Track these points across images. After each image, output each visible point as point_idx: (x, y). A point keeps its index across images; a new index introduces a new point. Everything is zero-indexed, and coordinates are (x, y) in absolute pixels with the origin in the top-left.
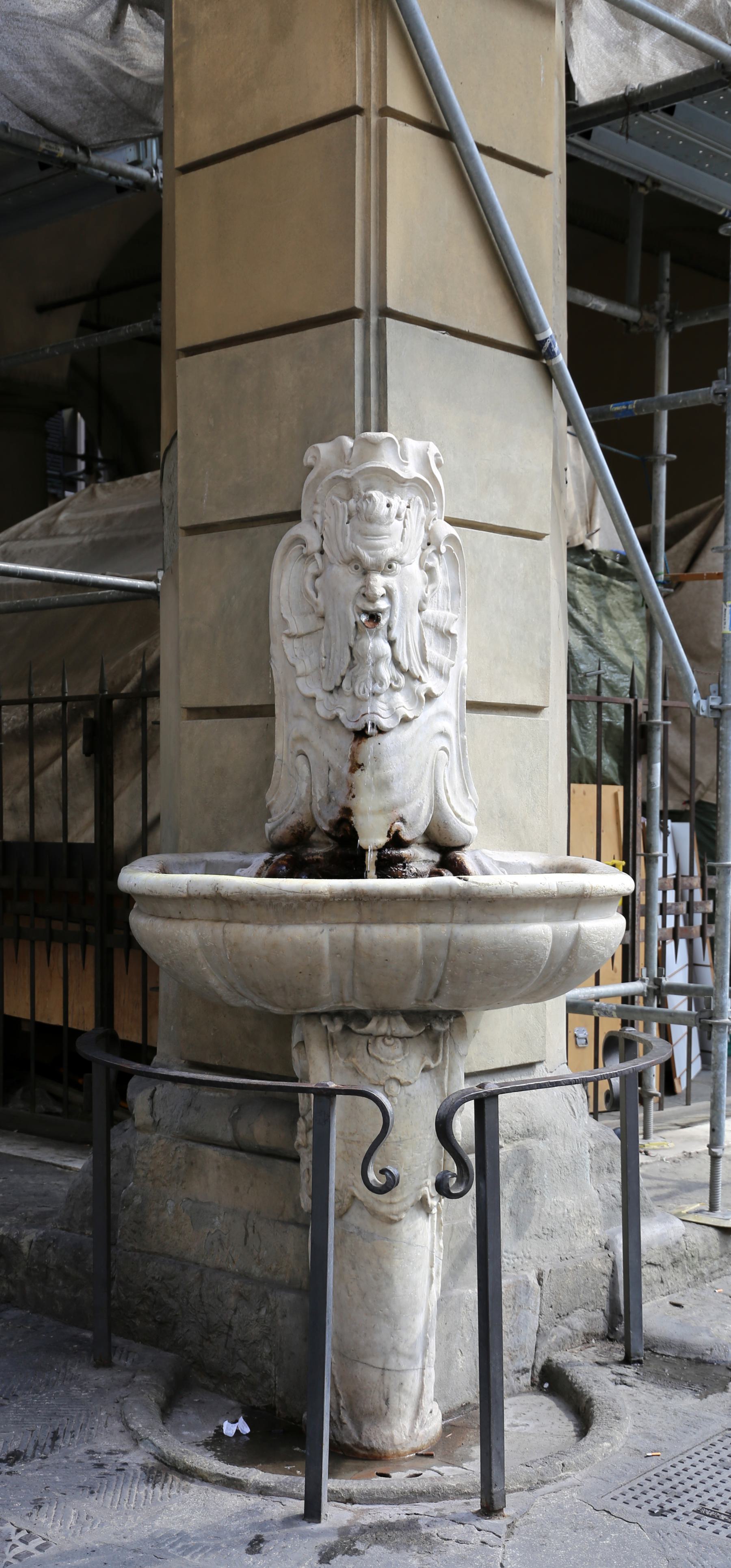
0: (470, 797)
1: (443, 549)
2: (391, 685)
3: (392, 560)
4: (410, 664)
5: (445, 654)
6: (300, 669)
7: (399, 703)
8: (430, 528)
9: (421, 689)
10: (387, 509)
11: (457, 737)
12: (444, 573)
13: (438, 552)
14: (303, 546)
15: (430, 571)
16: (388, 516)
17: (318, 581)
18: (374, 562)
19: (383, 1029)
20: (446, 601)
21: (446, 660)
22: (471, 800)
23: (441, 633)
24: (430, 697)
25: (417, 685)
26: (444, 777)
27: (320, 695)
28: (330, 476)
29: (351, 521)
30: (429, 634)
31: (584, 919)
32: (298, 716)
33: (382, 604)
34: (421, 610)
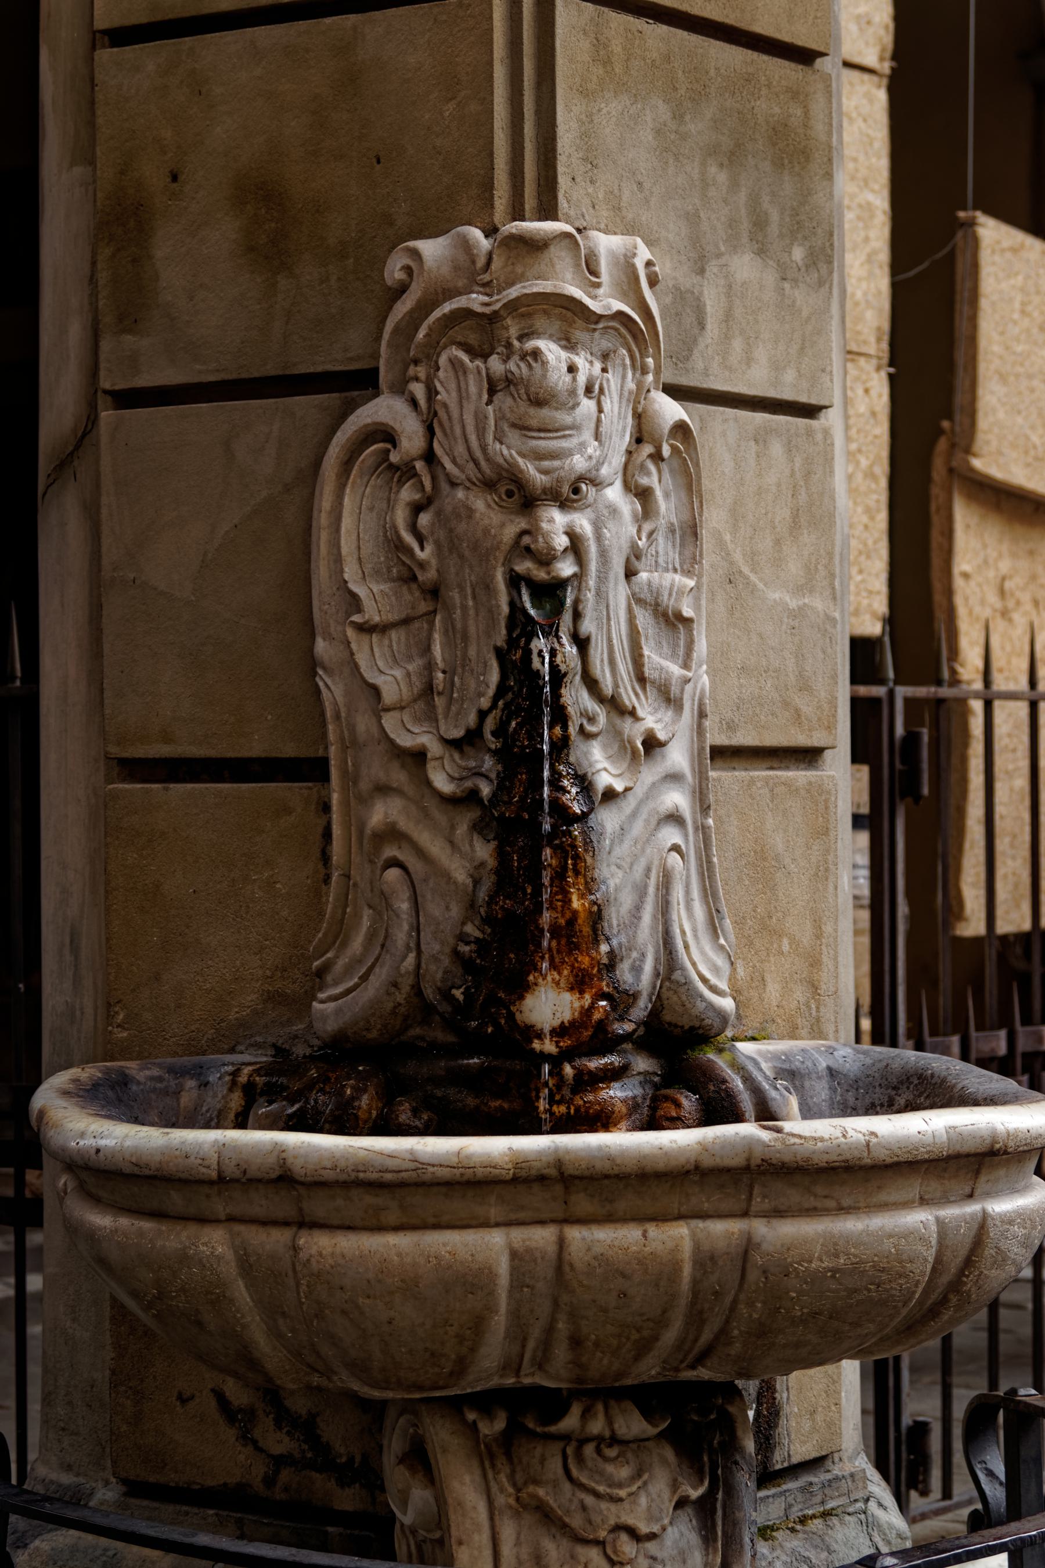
0: (722, 941)
1: (666, 451)
2: (581, 726)
3: (581, 478)
4: (616, 686)
5: (673, 656)
6: (389, 695)
8: (640, 410)
9: (636, 733)
10: (568, 378)
11: (695, 822)
12: (667, 495)
13: (657, 457)
14: (389, 446)
15: (644, 495)
16: (573, 393)
17: (424, 519)
18: (548, 485)
19: (597, 1426)
20: (671, 553)
21: (675, 670)
22: (722, 947)
23: (665, 615)
24: (652, 744)
25: (627, 726)
26: (679, 904)
27: (435, 748)
28: (447, 307)
29: (495, 398)
30: (644, 619)
31: (989, 1195)
32: (383, 790)
33: (566, 569)
34: (630, 574)
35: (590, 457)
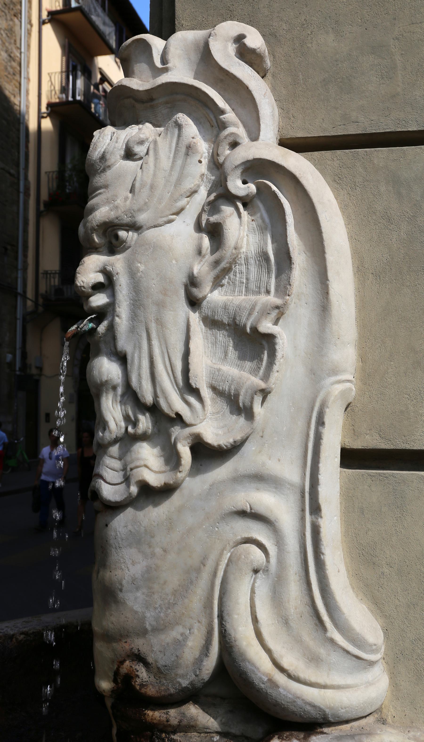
4: (156, 396)
7: (138, 459)
20: (265, 278)
35: (117, 207)
